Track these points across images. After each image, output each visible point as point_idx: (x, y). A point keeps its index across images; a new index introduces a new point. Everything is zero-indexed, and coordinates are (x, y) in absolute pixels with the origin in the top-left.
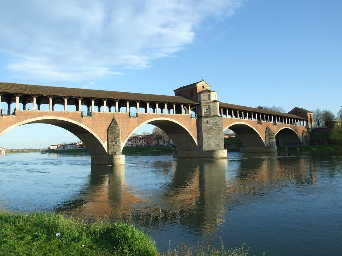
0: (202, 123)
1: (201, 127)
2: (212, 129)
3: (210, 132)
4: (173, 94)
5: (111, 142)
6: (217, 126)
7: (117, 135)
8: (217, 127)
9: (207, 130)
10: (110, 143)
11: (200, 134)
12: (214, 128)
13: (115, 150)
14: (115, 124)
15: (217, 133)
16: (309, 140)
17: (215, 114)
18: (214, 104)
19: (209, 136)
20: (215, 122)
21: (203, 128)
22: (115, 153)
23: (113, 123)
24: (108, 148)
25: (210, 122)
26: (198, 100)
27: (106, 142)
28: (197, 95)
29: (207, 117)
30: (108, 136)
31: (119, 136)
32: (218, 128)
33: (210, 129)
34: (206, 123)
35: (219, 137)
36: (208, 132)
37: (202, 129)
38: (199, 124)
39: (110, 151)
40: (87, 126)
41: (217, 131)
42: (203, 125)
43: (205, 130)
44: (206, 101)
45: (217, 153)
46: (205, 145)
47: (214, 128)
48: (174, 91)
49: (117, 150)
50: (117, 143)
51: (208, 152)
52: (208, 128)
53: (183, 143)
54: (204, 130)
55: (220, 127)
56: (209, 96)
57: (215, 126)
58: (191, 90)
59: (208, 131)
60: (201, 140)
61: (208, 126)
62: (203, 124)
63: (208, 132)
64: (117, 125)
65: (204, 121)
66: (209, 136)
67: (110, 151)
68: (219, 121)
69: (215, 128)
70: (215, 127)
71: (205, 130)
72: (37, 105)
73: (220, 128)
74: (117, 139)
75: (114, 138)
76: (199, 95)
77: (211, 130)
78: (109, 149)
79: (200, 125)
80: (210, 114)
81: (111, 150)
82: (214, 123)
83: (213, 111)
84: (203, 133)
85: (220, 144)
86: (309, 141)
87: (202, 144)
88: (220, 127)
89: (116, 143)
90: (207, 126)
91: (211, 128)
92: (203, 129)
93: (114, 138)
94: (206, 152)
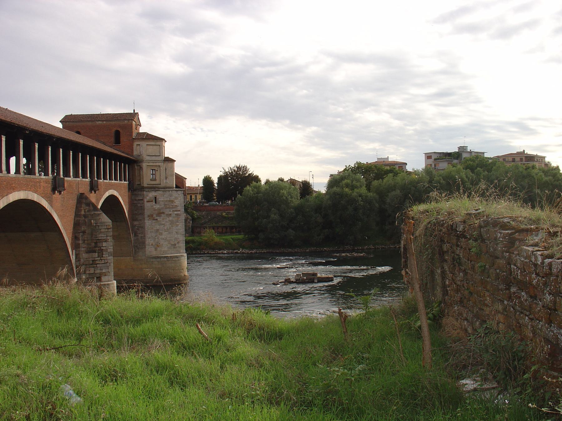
0: (145, 200)
1: (142, 208)
2: (163, 213)
3: (158, 220)
6: (173, 208)
7: (101, 236)
8: (174, 209)
9: (154, 216)
11: (136, 223)
12: (167, 211)
13: (98, 271)
14: (91, 208)
15: (172, 223)
16: (190, 226)
17: (168, 185)
18: (170, 164)
19: (158, 227)
20: (170, 201)
21: (146, 211)
22: (97, 278)
23: (83, 205)
25: (160, 199)
26: (135, 153)
28: (133, 142)
29: (154, 188)
31: (108, 238)
32: (176, 213)
33: (160, 214)
34: (152, 201)
35: (177, 229)
36: (157, 219)
37: (143, 214)
38: (135, 202)
41: (174, 217)
42: (147, 205)
43: (151, 216)
44: (152, 157)
45: (178, 260)
46: (149, 245)
47: (167, 211)
48: (60, 122)
49: (104, 271)
51: (159, 260)
52: (156, 212)
54: (149, 216)
55: (179, 211)
56: (161, 148)
57: (169, 208)
58: (115, 129)
59: (157, 218)
60: (140, 235)
61: (157, 207)
62: (146, 203)
63: (157, 219)
65: (148, 198)
66: (158, 227)
68: (176, 198)
69: (170, 213)
70: (168, 210)
71: (151, 216)
73: (179, 212)
74: (104, 244)
75: (96, 243)
76: (136, 143)
77: (162, 215)
79: (139, 205)
80: (160, 184)
81: (88, 272)
82: (166, 203)
83: (166, 178)
84: (145, 221)
85: (178, 243)
86: (189, 228)
87: (144, 243)
88: (179, 211)
89: (101, 255)
90: (155, 207)
91: (161, 212)
92: (147, 213)
93: (96, 243)
94: (154, 260)
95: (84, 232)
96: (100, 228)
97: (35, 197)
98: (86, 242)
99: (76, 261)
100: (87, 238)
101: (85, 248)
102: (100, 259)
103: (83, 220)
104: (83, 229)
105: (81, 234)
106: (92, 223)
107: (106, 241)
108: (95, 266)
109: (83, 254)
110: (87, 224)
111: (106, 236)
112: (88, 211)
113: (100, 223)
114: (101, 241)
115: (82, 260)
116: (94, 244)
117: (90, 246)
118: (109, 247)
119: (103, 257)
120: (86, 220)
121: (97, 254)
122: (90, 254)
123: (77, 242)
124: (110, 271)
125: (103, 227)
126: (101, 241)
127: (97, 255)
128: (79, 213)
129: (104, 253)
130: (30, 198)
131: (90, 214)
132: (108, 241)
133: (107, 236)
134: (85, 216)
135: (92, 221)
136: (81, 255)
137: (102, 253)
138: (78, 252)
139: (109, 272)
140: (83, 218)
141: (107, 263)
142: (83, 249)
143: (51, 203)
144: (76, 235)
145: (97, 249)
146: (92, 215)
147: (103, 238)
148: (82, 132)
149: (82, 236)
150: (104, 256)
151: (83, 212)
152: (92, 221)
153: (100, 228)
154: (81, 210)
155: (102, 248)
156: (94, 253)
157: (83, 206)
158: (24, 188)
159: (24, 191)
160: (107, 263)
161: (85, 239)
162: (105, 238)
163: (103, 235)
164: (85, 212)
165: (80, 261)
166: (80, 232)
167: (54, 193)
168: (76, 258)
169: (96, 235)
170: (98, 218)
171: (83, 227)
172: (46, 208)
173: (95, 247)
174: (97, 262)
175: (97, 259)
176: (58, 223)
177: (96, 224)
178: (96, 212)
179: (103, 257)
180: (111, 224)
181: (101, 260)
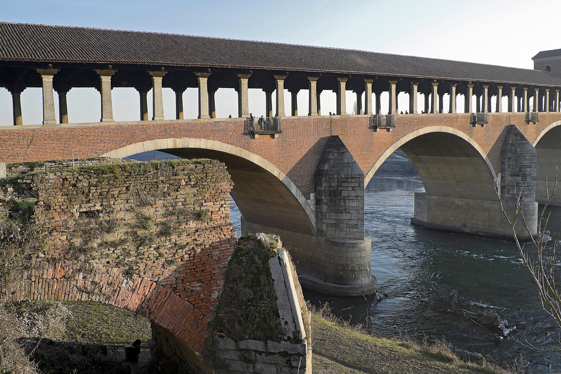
4: (530, 66)
5: (512, 175)
7: (526, 163)
10: (508, 178)
14: (519, 137)
24: (503, 187)
27: (500, 175)
30: (503, 163)
39: (508, 192)
40: (479, 144)
48: (532, 59)
50: (526, 178)
53: (557, 167)
64: (525, 142)
67: (508, 192)
72: (496, 109)
74: (528, 170)
78: (506, 190)
95: (510, 158)
96: (525, 155)
97: (450, 130)
98: (511, 167)
99: (501, 182)
100: (512, 163)
101: (510, 171)
102: (523, 182)
103: (510, 148)
104: (509, 156)
105: (507, 160)
106: (517, 151)
107: (529, 167)
108: (519, 187)
109: (508, 177)
110: (513, 152)
111: (530, 162)
112: (515, 141)
113: (525, 151)
114: (525, 167)
115: (506, 182)
116: (518, 169)
117: (514, 171)
118: (534, 173)
119: (526, 180)
120: (512, 149)
121: (520, 178)
122: (515, 177)
123: (503, 166)
124: (532, 193)
125: (528, 155)
126: (525, 167)
127: (521, 179)
128: (507, 142)
129: (527, 177)
130: (443, 131)
131: (517, 143)
132: (532, 167)
133: (531, 163)
134: (512, 145)
135: (518, 149)
136: (506, 177)
137: (525, 177)
138: (503, 176)
139: (531, 194)
140: (510, 147)
141: (529, 186)
142: (507, 173)
143: (470, 135)
144: (503, 160)
145: (522, 173)
146: (519, 143)
147: (527, 164)
148: (551, 66)
149: (508, 161)
150: (527, 180)
151: (511, 141)
152: (518, 149)
153: (525, 155)
154: (509, 140)
155: (526, 173)
156: (518, 177)
157: (511, 136)
158: (438, 124)
159: (437, 126)
160: (529, 186)
161: (511, 164)
162: (529, 164)
163: (527, 162)
164: (512, 141)
165: (505, 182)
166: (506, 158)
167: (474, 126)
168: (502, 180)
169: (521, 162)
170: (524, 146)
171: (509, 154)
172: (464, 138)
173: (519, 172)
174: (520, 185)
175: (520, 182)
176: (478, 151)
177: (520, 152)
178: (523, 142)
179: (526, 180)
180: (536, 152)
181: (525, 183)
